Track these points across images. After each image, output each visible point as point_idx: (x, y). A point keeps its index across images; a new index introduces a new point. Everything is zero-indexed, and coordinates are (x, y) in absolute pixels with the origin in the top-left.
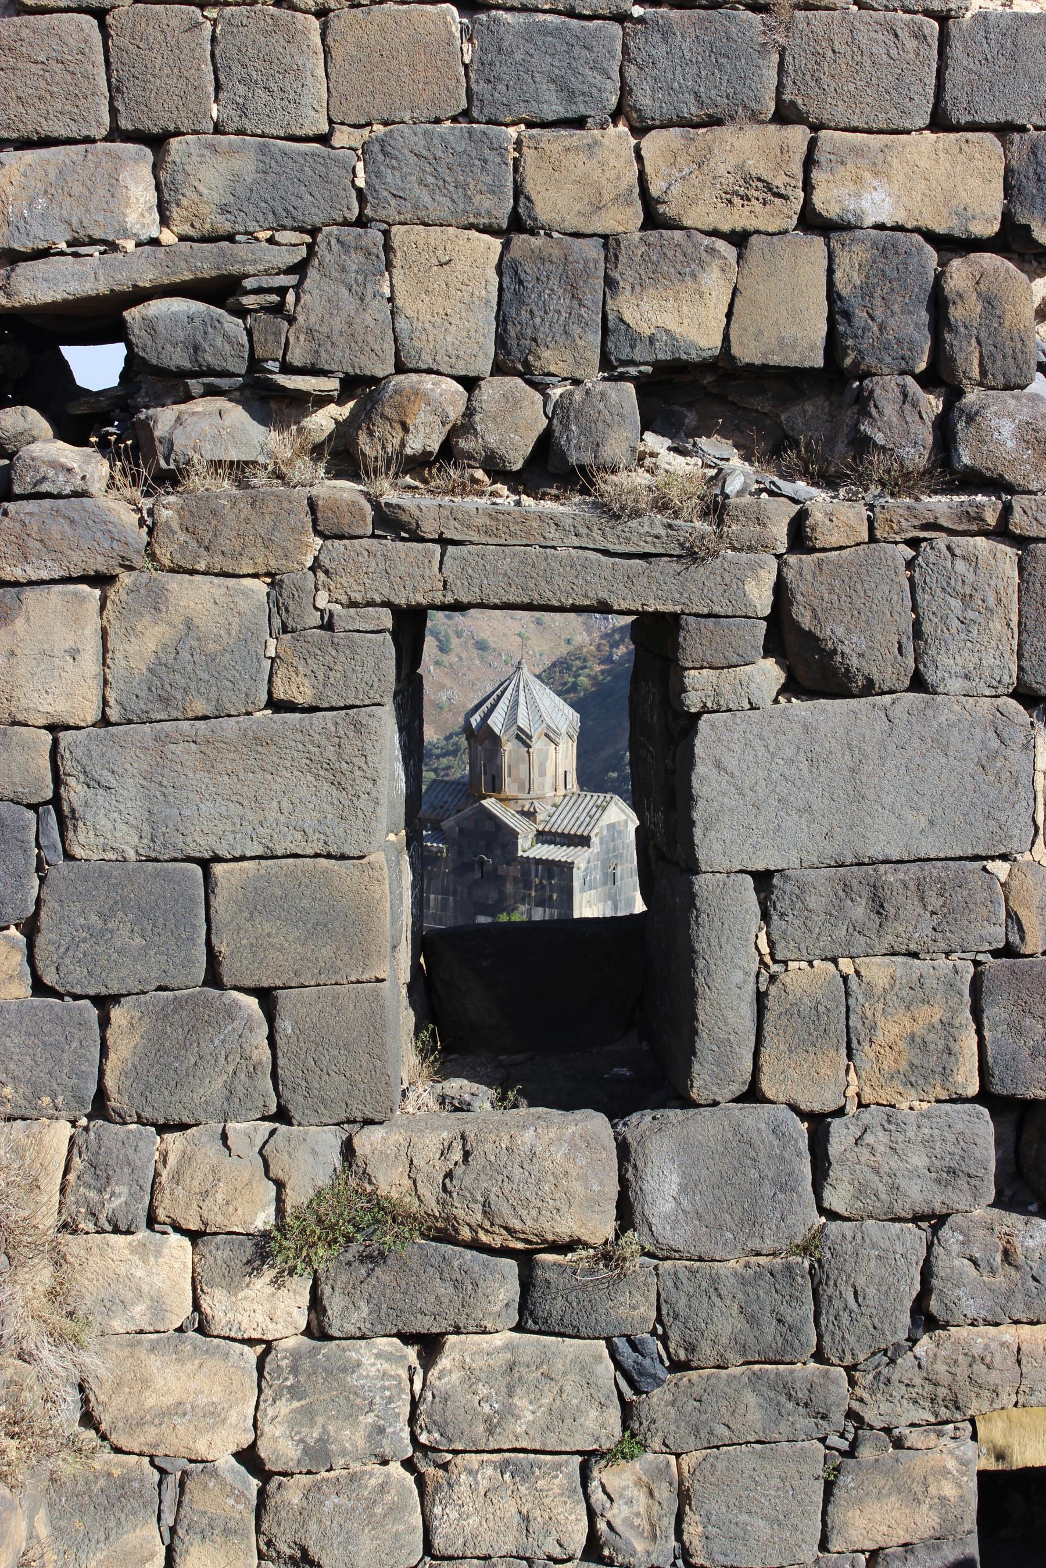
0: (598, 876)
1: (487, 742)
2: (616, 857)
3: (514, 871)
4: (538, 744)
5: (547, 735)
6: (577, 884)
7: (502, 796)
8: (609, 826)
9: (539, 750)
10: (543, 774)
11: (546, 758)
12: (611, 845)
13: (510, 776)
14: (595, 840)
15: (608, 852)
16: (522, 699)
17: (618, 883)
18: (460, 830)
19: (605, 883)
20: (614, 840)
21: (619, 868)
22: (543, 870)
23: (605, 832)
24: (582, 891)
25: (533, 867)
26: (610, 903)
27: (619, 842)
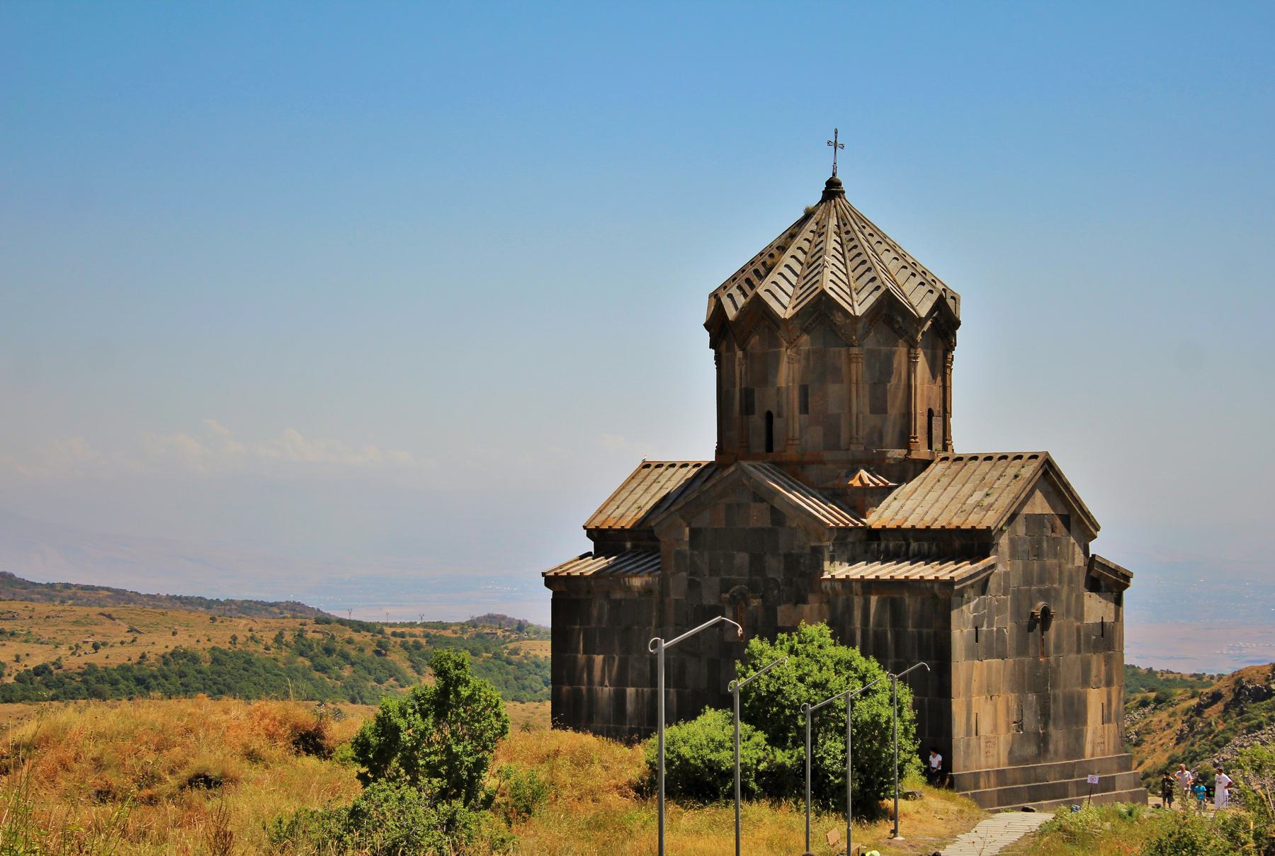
0: (1006, 625)
1: (755, 340)
2: (1045, 595)
5: (890, 321)
6: (960, 634)
7: (791, 453)
8: (1028, 517)
9: (871, 353)
10: (879, 407)
11: (884, 371)
12: (1036, 566)
13: (804, 408)
14: (1004, 541)
15: (1027, 580)
16: (832, 243)
17: (1052, 658)
18: (695, 533)
19: (1022, 650)
20: (1038, 554)
21: (1054, 623)
22: (881, 604)
23: (1020, 528)
24: (972, 654)
25: (858, 601)
26: (1032, 697)
27: (1050, 562)
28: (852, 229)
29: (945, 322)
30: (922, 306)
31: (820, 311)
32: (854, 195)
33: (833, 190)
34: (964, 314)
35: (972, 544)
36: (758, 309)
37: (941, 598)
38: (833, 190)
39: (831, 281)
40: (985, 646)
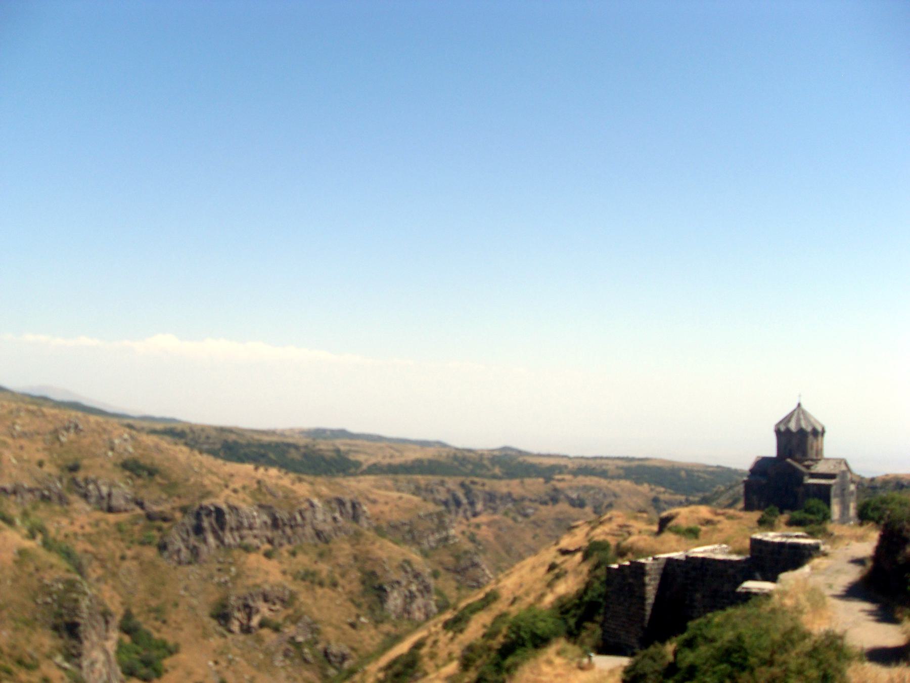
0: (838, 492)
3: (802, 489)
4: (811, 437)
10: (812, 448)
16: (802, 417)
28: (804, 412)
29: (823, 432)
30: (820, 429)
31: (802, 432)
32: (804, 406)
33: (799, 405)
34: (827, 429)
35: (832, 476)
36: (788, 431)
37: (828, 487)
38: (799, 405)
39: (803, 424)
40: (836, 496)
